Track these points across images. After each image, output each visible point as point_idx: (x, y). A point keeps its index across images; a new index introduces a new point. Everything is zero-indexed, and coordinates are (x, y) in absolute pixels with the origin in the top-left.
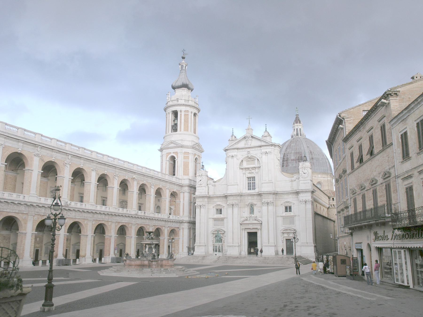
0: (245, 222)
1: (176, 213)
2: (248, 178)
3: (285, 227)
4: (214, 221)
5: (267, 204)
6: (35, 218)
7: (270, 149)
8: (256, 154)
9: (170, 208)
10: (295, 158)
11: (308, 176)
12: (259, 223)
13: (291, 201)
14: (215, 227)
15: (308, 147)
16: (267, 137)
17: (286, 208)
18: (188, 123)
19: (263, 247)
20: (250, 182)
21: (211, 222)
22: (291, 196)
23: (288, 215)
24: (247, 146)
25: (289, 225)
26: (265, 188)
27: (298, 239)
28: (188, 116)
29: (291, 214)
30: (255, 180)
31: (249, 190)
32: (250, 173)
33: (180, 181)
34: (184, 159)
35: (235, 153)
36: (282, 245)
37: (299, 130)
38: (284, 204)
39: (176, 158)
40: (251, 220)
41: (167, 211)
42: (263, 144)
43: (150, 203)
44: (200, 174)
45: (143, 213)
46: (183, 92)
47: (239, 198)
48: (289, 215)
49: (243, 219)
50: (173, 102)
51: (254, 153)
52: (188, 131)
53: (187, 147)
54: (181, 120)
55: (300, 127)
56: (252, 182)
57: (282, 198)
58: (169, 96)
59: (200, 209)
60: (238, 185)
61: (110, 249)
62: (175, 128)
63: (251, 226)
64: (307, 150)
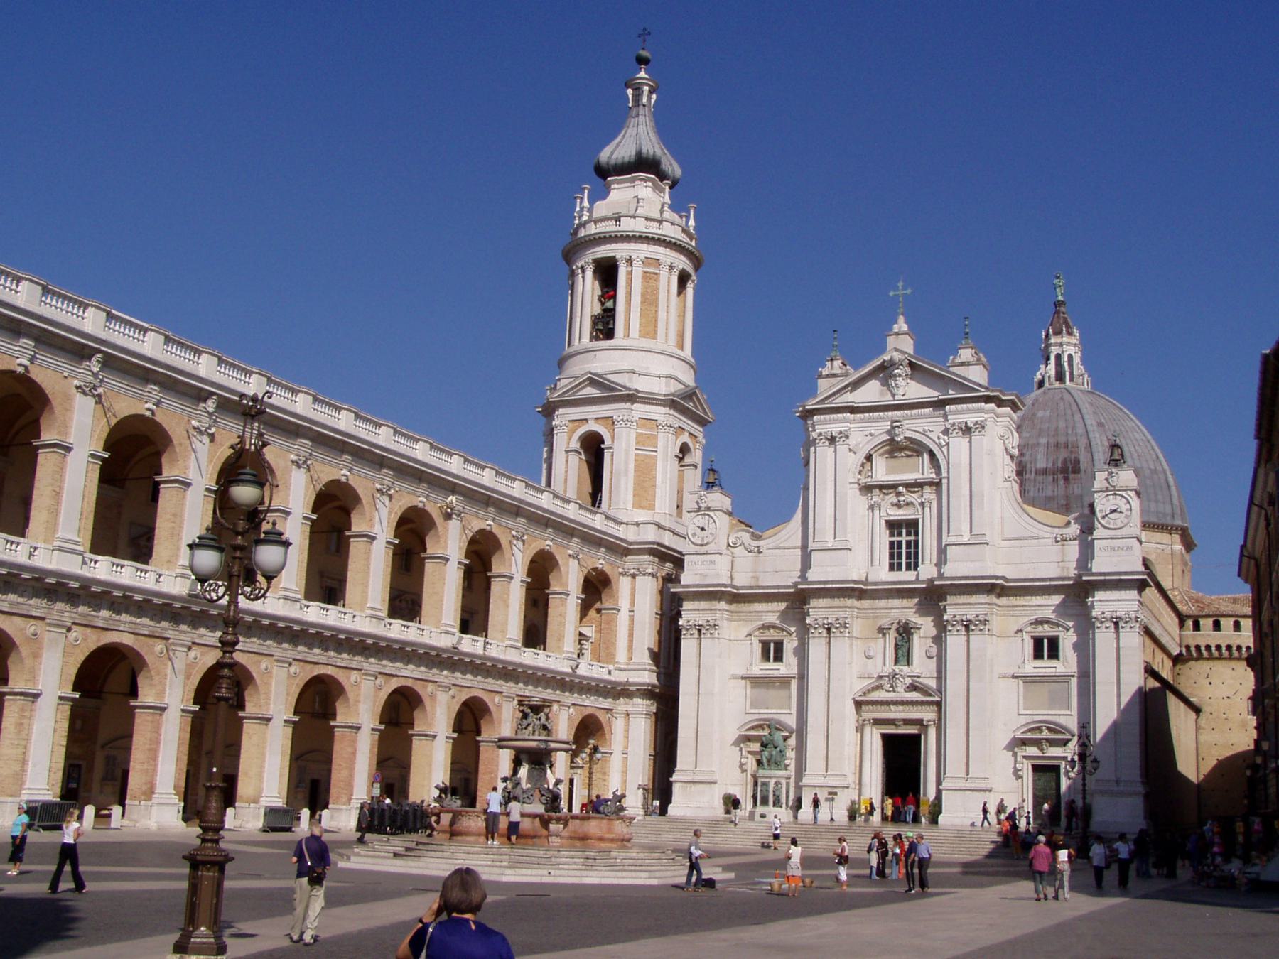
0: (876, 695)
1: (604, 653)
2: (894, 526)
3: (1029, 719)
4: (752, 687)
6: (72, 635)
9: (581, 634)
10: (1050, 465)
11: (1125, 521)
14: (756, 711)
15: (1101, 425)
16: (971, 367)
17: (1038, 642)
18: (657, 306)
19: (944, 792)
20: (899, 539)
23: (1044, 670)
24: (887, 399)
25: (1046, 712)
27: (1095, 761)
30: (916, 534)
32: (898, 505)
33: (623, 527)
34: (637, 443)
35: (843, 427)
37: (1065, 358)
38: (1029, 629)
39: (608, 442)
41: (570, 644)
43: (508, 606)
45: (480, 644)
48: (1047, 670)
50: (599, 225)
51: (915, 426)
52: (655, 337)
53: (651, 400)
54: (629, 293)
55: (1069, 350)
56: (904, 539)
57: (1023, 606)
58: (586, 204)
59: (700, 638)
61: (351, 776)
63: (897, 713)
64: (1097, 435)
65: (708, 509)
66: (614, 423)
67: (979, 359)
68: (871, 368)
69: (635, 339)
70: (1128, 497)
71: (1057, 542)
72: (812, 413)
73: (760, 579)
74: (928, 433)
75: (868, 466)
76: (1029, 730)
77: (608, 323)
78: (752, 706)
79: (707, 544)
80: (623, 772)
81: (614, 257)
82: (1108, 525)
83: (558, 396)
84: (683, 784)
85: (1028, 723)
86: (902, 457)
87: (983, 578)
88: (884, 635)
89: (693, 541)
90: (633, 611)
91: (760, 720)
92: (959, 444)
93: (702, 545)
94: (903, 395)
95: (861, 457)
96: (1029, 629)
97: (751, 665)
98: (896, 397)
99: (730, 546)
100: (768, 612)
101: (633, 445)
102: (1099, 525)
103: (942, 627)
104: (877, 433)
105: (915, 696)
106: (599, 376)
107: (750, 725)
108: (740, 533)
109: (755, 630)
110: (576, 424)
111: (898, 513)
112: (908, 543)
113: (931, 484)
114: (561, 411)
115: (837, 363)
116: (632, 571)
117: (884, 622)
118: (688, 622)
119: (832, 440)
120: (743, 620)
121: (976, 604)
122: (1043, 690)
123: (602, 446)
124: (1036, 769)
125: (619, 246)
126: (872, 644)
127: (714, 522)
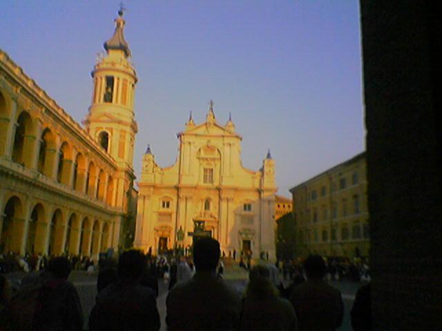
21: (155, 217)
24: (207, 133)
26: (227, 183)
32: (208, 164)
36: (239, 248)
39: (110, 134)
42: (227, 134)
46: (116, 56)
47: (193, 190)
51: (217, 143)
62: (108, 98)
92: (227, 149)
95: (197, 149)
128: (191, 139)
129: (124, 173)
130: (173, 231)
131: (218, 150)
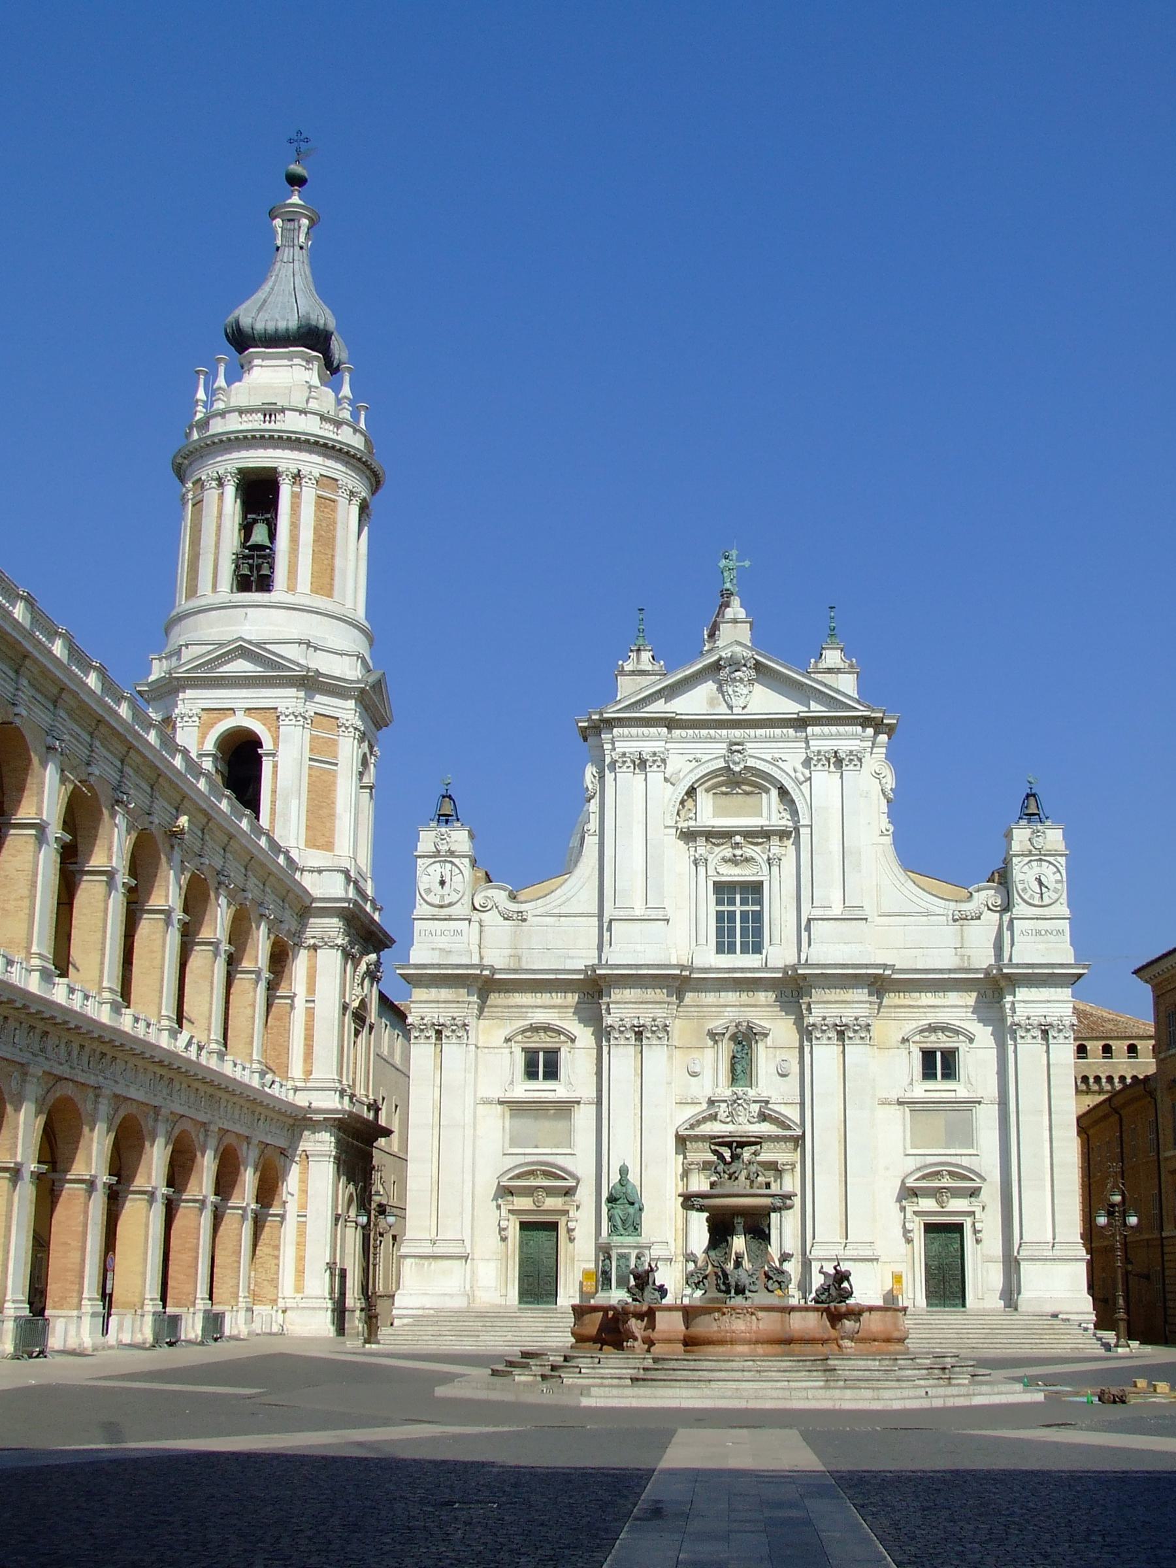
2: (723, 889)
3: (920, 1161)
4: (511, 1116)
5: (833, 1035)
7: (858, 742)
8: (773, 762)
12: (781, 1132)
13: (957, 1023)
17: (928, 1056)
20: (731, 908)
21: (495, 1123)
22: (953, 998)
28: (334, 510)
29: (958, 1090)
30: (759, 902)
31: (720, 950)
32: (734, 861)
34: (311, 750)
35: (658, 746)
38: (917, 1038)
39: (267, 745)
40: (741, 1119)
42: (817, 708)
44: (443, 848)
49: (690, 1112)
54: (295, 526)
56: (738, 908)
60: (668, 920)
65: (452, 853)
66: (278, 717)
67: (851, 666)
68: (700, 666)
69: (304, 593)
70: (1058, 865)
71: (955, 920)
72: (610, 724)
73: (524, 959)
74: (780, 763)
75: (689, 804)
76: (923, 1177)
77: (259, 567)
78: (513, 1143)
79: (450, 905)
80: (298, 1244)
81: (276, 468)
82: (1031, 901)
83: (187, 671)
84: (417, 1260)
85: (919, 1169)
86: (737, 793)
87: (867, 966)
88: (716, 1042)
89: (429, 900)
90: (313, 1001)
91: (533, 1163)
92: (825, 781)
93: (441, 907)
94: (744, 708)
96: (917, 1038)
97: (512, 1083)
98: (735, 711)
99: (475, 909)
100: (537, 1007)
101: (307, 755)
102: (1020, 900)
103: (806, 1033)
104: (705, 758)
105: (766, 1128)
106: (257, 645)
107: (517, 1172)
108: (490, 891)
109: (517, 1034)
110: (214, 715)
111: (730, 873)
112: (744, 914)
113: (783, 834)
114: (190, 693)
115: (646, 656)
116: (312, 941)
117: (717, 1024)
118: (422, 1019)
119: (641, 764)
120: (498, 1018)
121: (853, 1002)
122: (939, 1121)
123: (260, 751)
124: (930, 1228)
125: (287, 454)
126: (695, 1054)
127: (461, 872)
128: (648, 741)
129: (335, 923)
130: (585, 1194)
131: (783, 792)
